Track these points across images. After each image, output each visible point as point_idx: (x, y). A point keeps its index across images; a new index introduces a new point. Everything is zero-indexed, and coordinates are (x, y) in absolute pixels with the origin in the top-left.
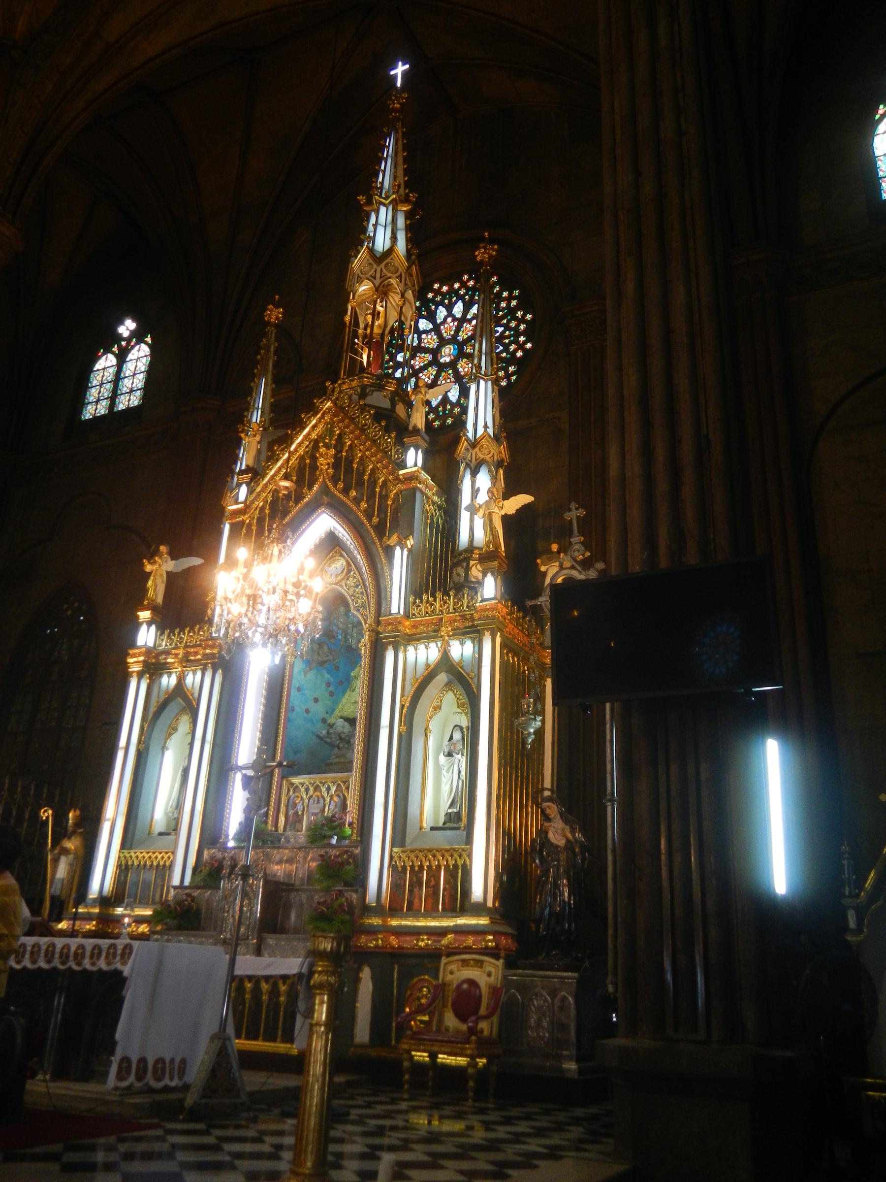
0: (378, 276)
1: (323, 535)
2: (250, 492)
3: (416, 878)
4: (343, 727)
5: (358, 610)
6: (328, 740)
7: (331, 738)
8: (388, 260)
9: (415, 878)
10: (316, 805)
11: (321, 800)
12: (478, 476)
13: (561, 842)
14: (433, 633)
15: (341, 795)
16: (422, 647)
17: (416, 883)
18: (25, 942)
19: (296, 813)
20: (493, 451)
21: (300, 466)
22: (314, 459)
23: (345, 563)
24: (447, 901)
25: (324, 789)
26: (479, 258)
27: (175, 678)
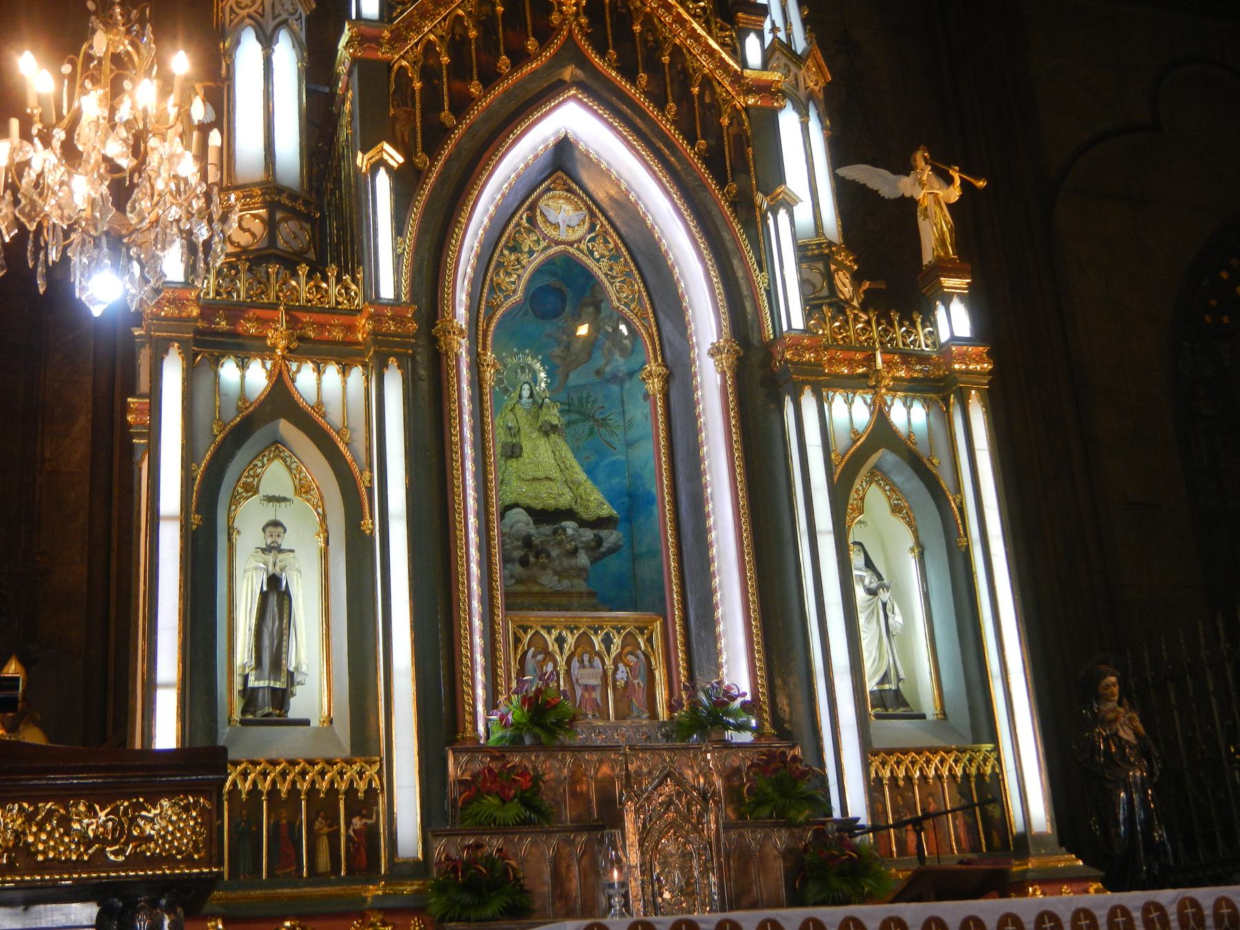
3: (902, 799)
4: (527, 524)
5: (626, 304)
9: (900, 799)
10: (588, 671)
11: (597, 661)
15: (639, 652)
18: (1122, 903)
20: (820, 83)
23: (585, 211)
24: (962, 835)
25: (597, 641)
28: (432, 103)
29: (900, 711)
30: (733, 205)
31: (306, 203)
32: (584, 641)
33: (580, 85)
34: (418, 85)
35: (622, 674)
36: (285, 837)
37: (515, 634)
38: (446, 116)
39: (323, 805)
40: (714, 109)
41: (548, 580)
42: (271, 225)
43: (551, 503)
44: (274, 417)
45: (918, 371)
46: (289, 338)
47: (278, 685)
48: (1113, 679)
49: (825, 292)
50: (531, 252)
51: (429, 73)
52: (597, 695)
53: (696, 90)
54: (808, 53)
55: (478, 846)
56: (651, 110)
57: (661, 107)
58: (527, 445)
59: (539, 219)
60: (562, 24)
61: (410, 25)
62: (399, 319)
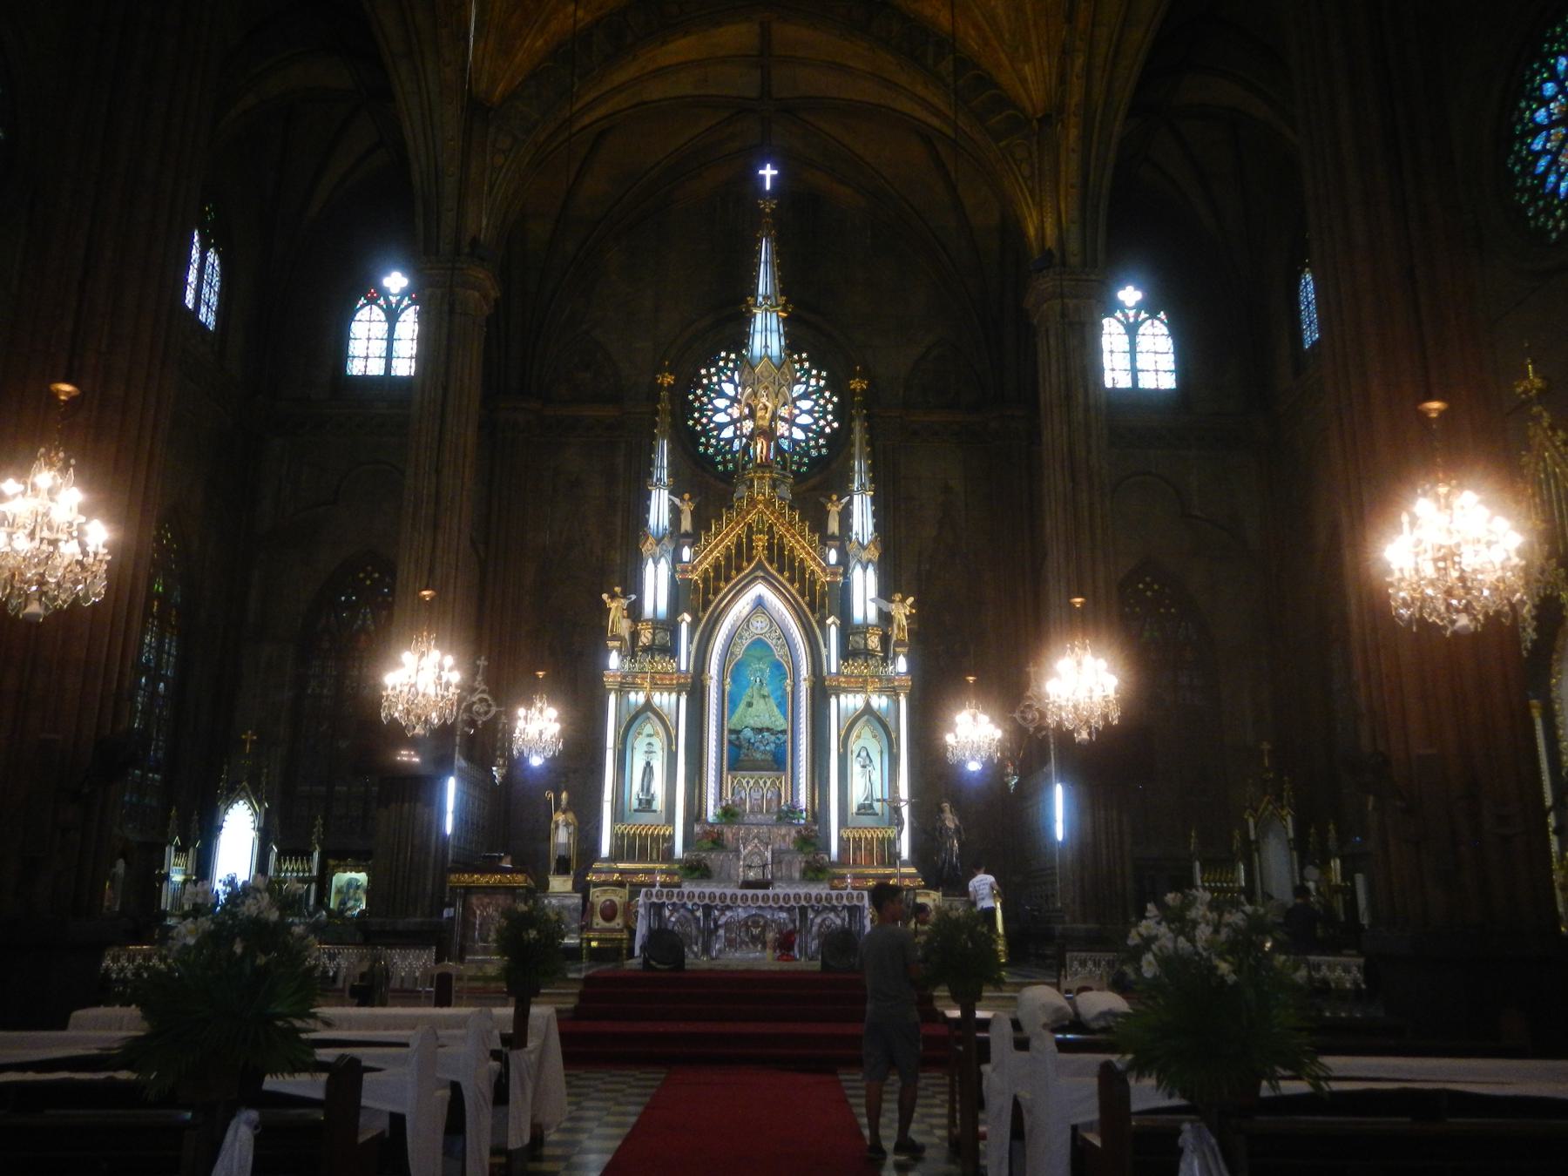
0: (777, 383)
1: (754, 598)
2: (696, 554)
6: (737, 743)
7: (740, 742)
8: (782, 370)
10: (757, 794)
12: (868, 571)
13: (952, 826)
14: (861, 686)
16: (850, 696)
17: (857, 848)
19: (741, 798)
21: (737, 542)
22: (750, 540)
25: (761, 783)
26: (852, 387)
27: (643, 696)
28: (706, 591)
29: (870, 812)
30: (817, 622)
31: (668, 625)
32: (757, 782)
33: (763, 578)
34: (701, 586)
35: (769, 795)
36: (643, 848)
37: (732, 779)
38: (711, 596)
39: (655, 839)
40: (813, 583)
41: (758, 756)
42: (654, 635)
43: (760, 726)
44: (646, 711)
45: (885, 684)
46: (651, 685)
47: (648, 798)
48: (946, 804)
49: (862, 647)
50: (746, 639)
51: (706, 580)
52: (760, 802)
53: (807, 576)
54: (869, 543)
55: (698, 855)
56: (788, 586)
57: (792, 584)
58: (755, 702)
59: (750, 626)
60: (757, 554)
61: (700, 563)
62: (686, 678)
